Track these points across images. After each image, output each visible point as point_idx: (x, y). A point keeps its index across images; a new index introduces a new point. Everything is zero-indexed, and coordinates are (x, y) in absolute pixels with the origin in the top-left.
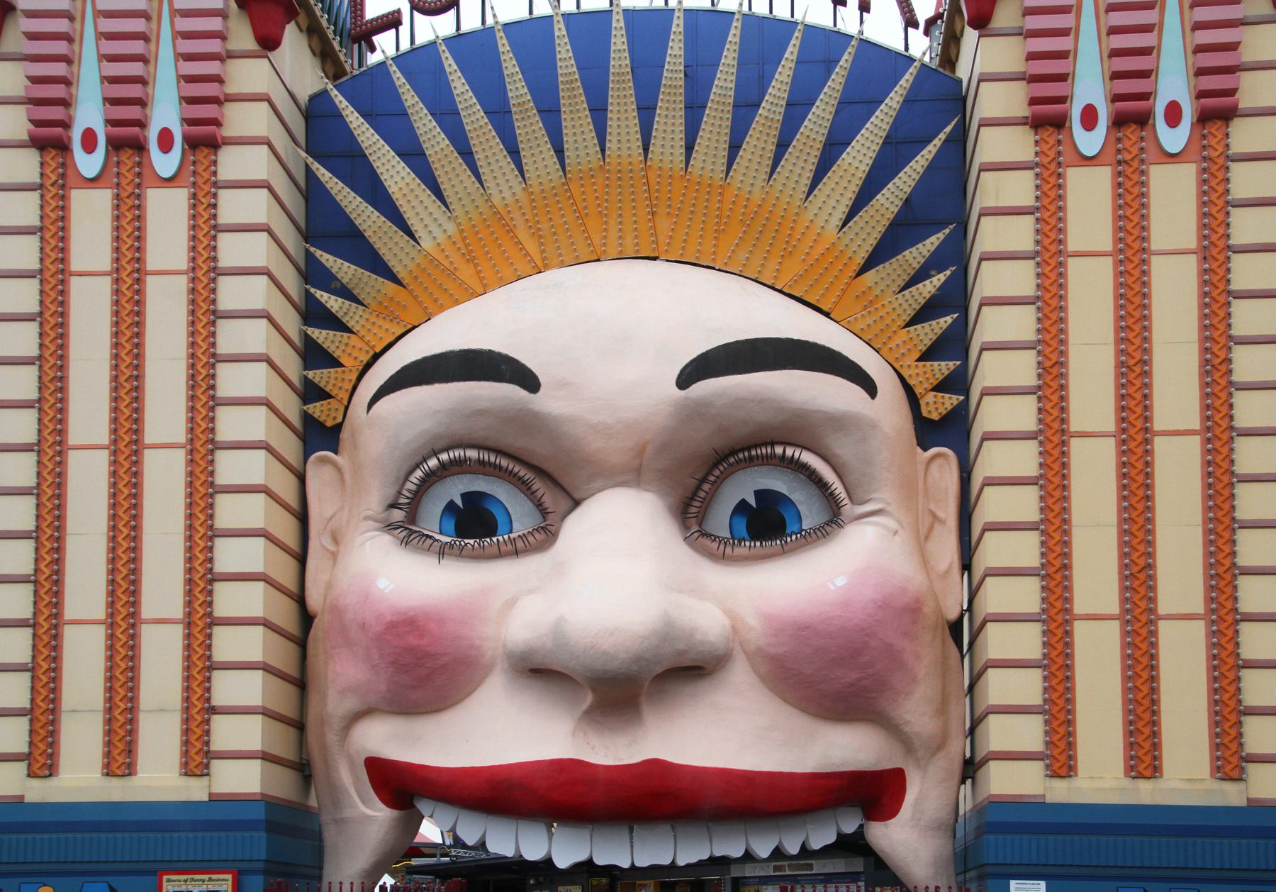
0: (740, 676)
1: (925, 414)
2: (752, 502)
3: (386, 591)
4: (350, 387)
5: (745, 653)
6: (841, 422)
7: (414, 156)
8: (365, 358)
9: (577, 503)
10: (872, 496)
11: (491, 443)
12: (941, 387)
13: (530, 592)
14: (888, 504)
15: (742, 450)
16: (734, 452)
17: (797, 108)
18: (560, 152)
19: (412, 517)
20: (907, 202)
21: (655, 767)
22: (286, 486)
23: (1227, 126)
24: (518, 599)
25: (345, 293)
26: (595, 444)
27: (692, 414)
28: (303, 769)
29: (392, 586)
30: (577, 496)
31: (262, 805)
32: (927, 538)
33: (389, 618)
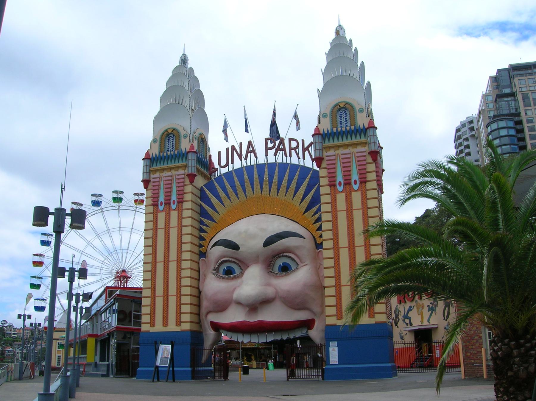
1: (317, 242)
6: (297, 247)
7: (218, 197)
8: (211, 238)
9: (248, 267)
11: (231, 257)
12: (320, 237)
16: (278, 255)
17: (290, 181)
18: (245, 193)
19: (218, 272)
20: (313, 197)
21: (261, 322)
22: (195, 266)
23: (366, 184)
25: (206, 225)
28: (199, 323)
31: (189, 333)
32: (319, 268)
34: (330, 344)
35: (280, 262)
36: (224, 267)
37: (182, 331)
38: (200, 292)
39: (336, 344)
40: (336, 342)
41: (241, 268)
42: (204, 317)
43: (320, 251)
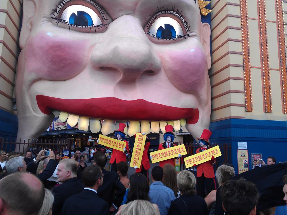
0: (162, 76)
2: (164, 27)
3: (50, 36)
5: (165, 70)
9: (113, 20)
10: (194, 31)
14: (198, 34)
24: (96, 45)
29: (53, 35)
30: (113, 17)
34: (238, 145)
35: (162, 22)
36: (73, 9)
38: (19, 49)
39: (246, 145)
40: (246, 143)
42: (25, 88)
43: (206, 25)
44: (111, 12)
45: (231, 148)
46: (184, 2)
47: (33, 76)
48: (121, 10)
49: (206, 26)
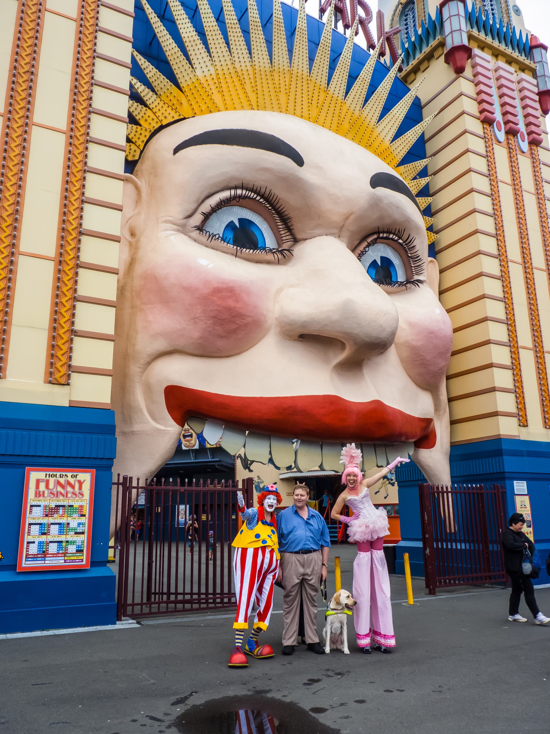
2: (379, 262)
4: (145, 140)
8: (157, 126)
9: (296, 241)
13: (292, 286)
15: (384, 232)
16: (378, 232)
26: (327, 206)
27: (376, 203)
30: (299, 236)
33: (216, 285)
34: (515, 488)
37: (74, 408)
39: (525, 488)
41: (279, 240)
44: (296, 226)
45: (505, 492)
46: (413, 221)
47: (161, 345)
48: (318, 226)
49: (431, 264)
